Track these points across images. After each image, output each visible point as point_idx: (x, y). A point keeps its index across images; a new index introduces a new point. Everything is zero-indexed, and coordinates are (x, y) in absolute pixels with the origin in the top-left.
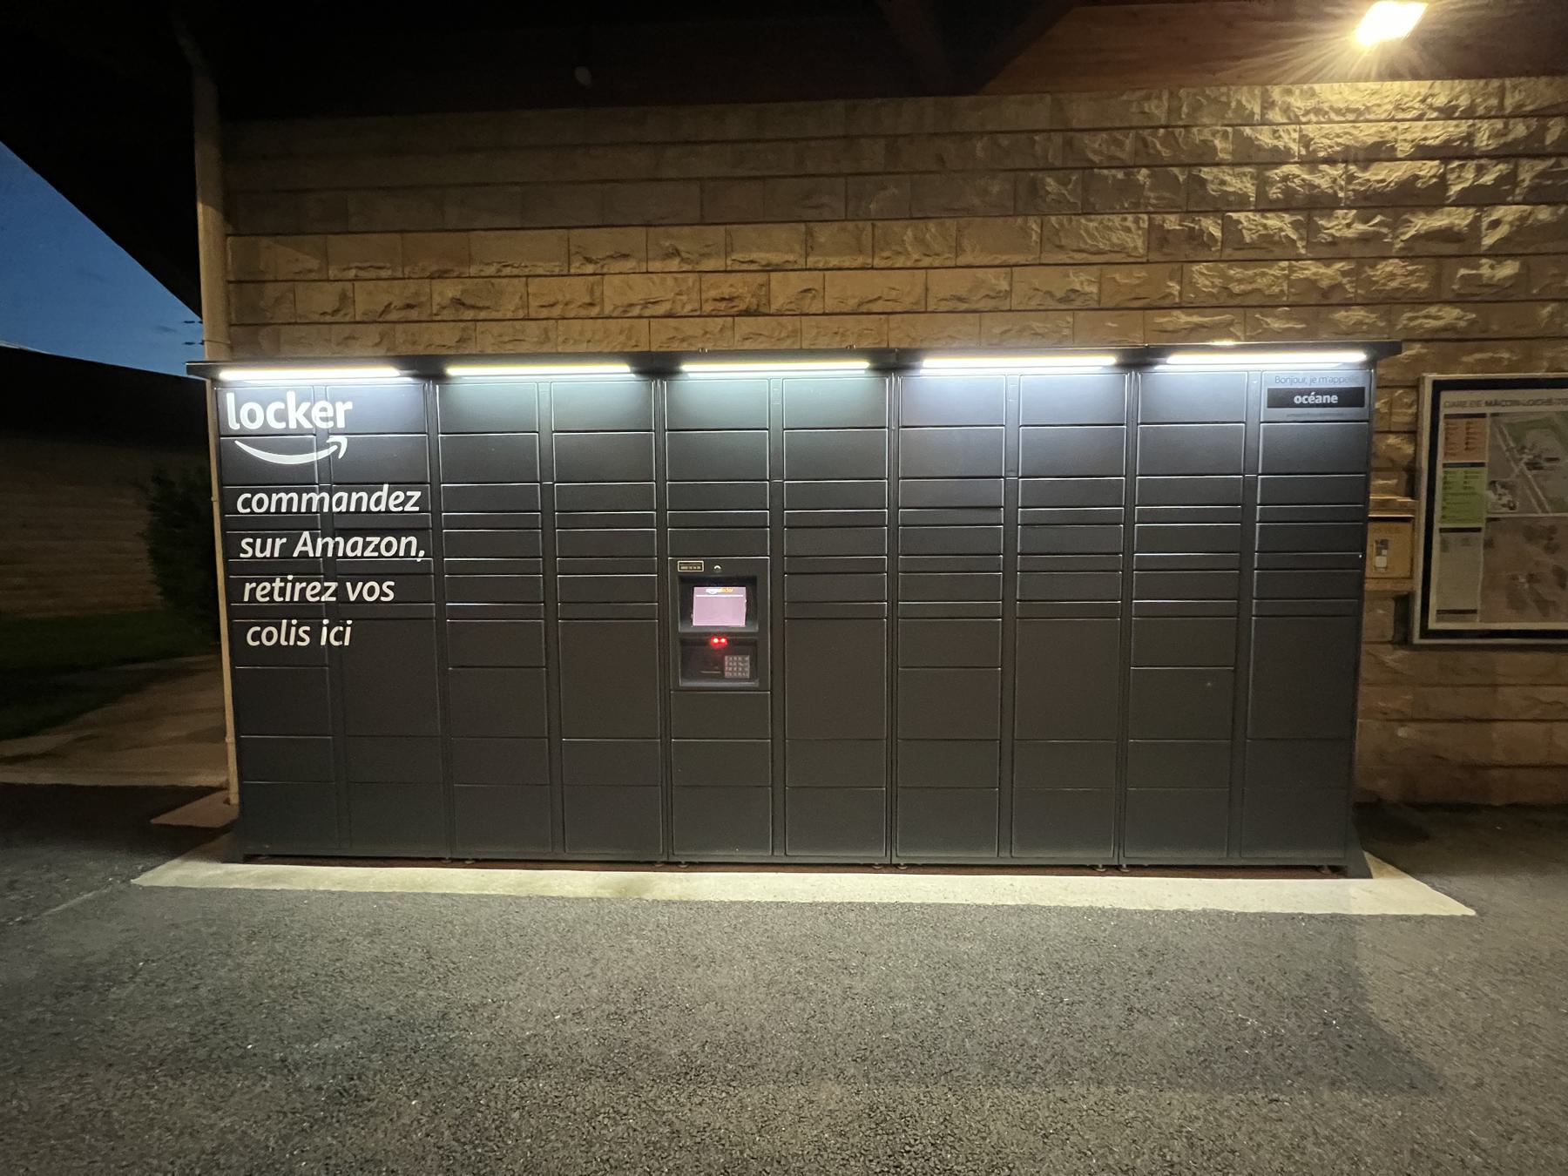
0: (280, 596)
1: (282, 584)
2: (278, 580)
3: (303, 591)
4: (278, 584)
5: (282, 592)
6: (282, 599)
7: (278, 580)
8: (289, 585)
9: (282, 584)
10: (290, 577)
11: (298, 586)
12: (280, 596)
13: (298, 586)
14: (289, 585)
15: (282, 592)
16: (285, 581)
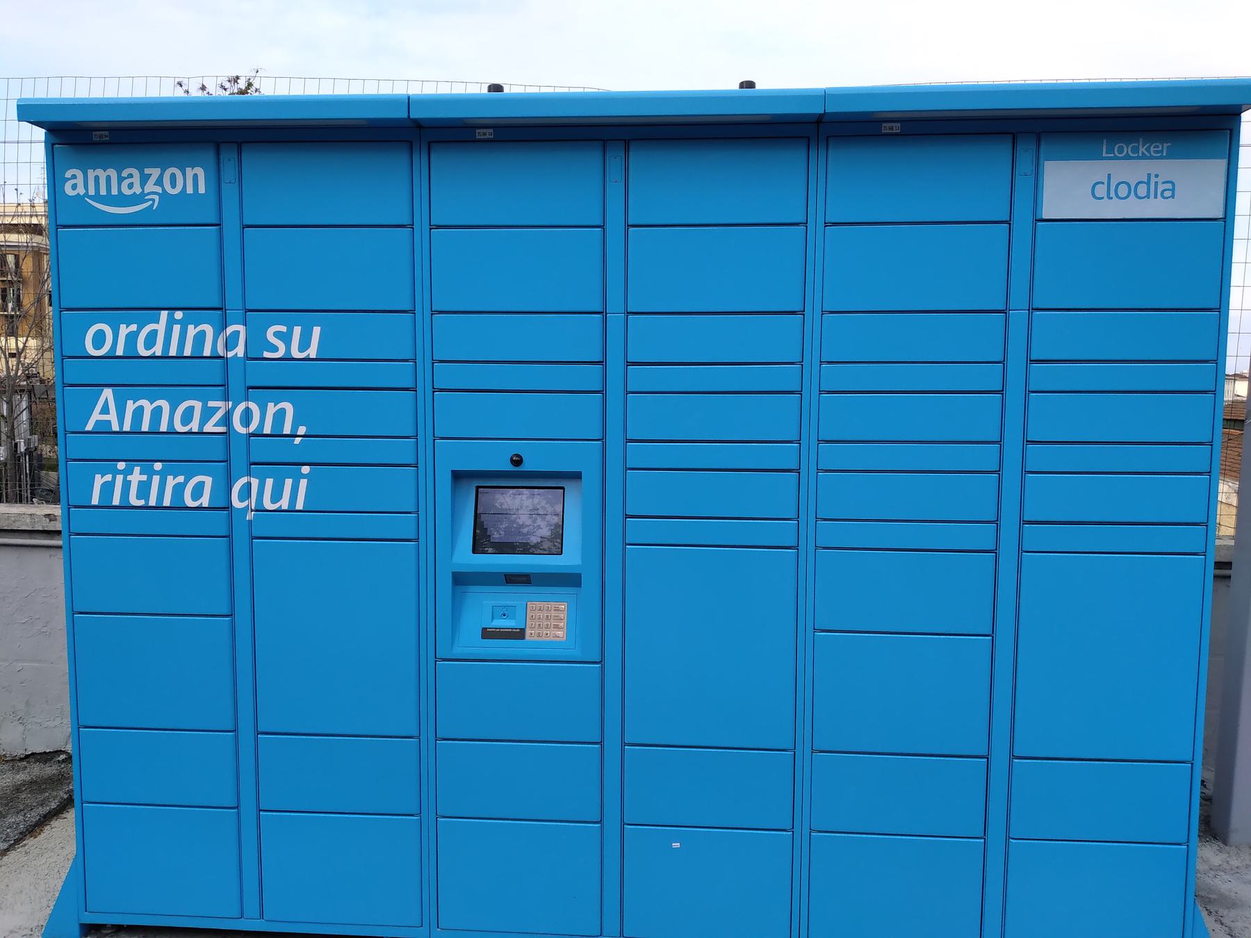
0: (138, 498)
1: (144, 478)
2: (137, 470)
3: (179, 490)
4: (136, 477)
5: (144, 489)
6: (141, 503)
7: (137, 470)
8: (156, 479)
9: (144, 478)
10: (158, 466)
11: (171, 482)
12: (138, 498)
13: (171, 482)
14: (156, 479)
15: (144, 489)
16: (151, 473)
